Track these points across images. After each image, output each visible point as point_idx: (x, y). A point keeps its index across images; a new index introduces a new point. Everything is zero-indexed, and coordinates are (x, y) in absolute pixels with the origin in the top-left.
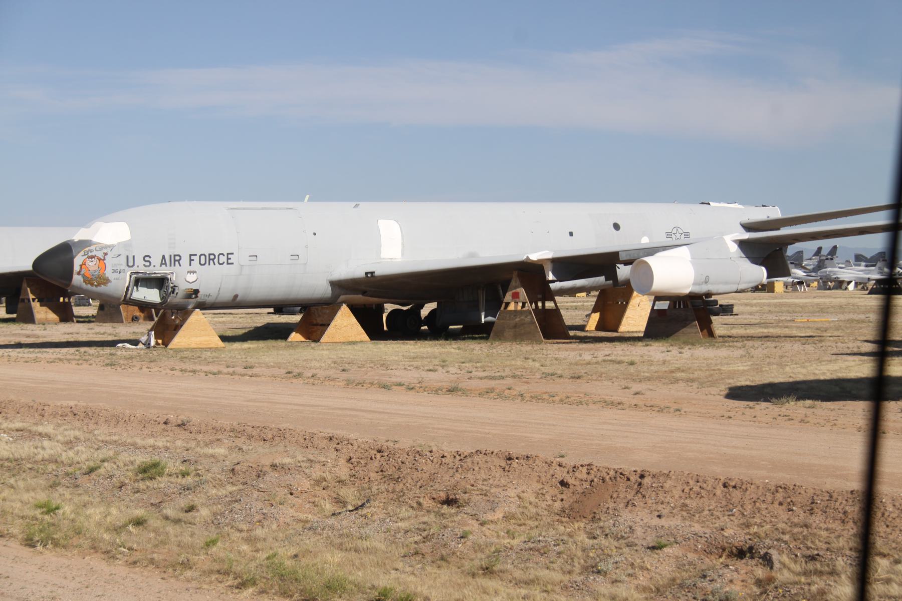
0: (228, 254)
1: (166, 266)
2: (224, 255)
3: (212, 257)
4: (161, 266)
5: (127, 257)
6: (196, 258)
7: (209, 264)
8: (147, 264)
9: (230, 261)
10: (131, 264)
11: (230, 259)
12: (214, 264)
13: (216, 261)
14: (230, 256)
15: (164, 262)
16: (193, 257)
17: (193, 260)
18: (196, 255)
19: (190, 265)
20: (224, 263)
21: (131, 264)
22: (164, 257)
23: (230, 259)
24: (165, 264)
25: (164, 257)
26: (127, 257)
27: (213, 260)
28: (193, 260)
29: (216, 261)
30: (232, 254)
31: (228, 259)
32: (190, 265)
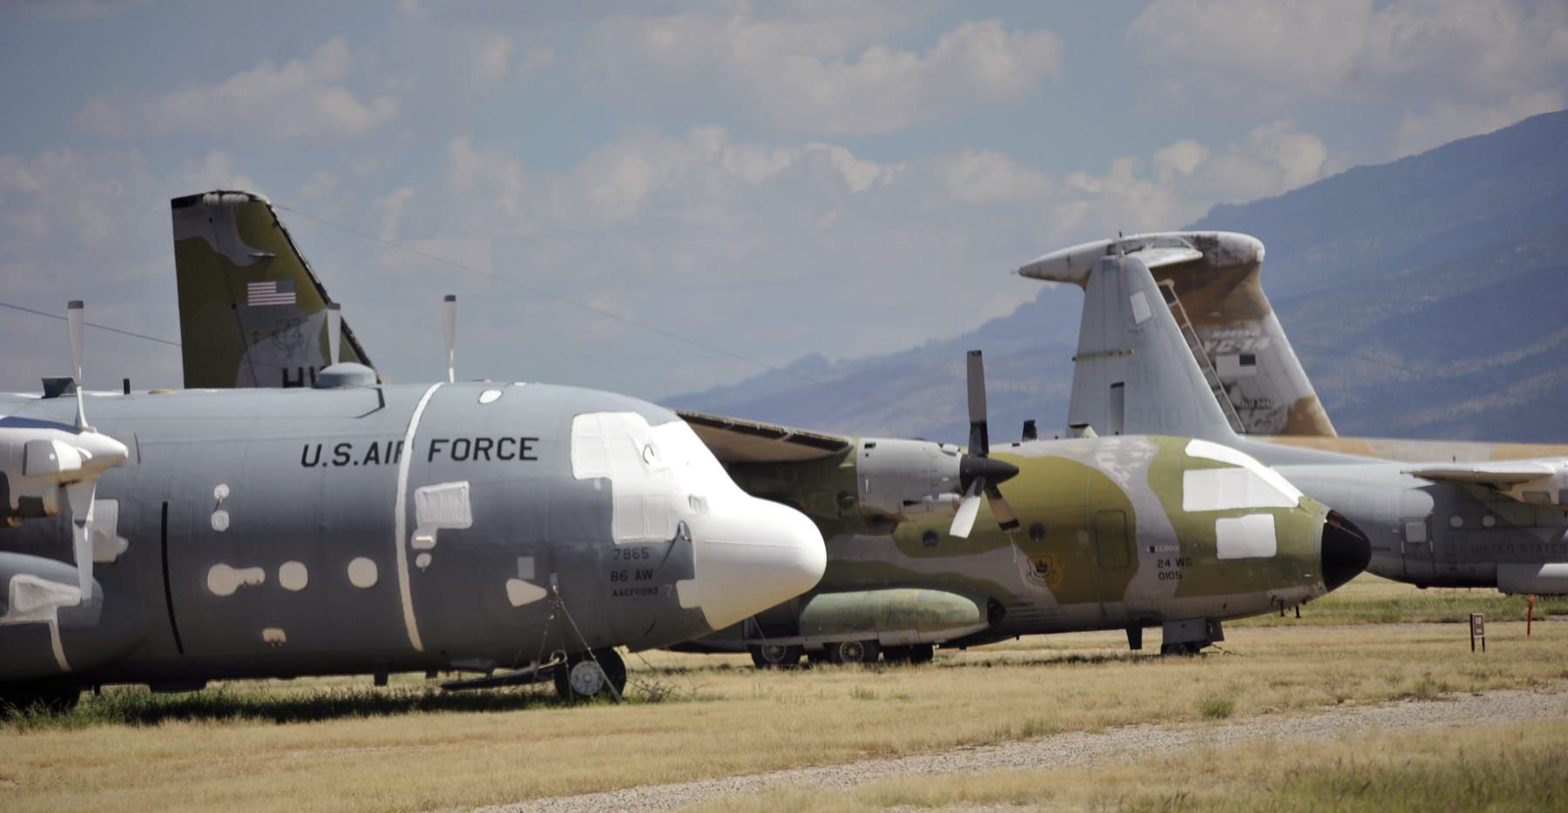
0: (523, 440)
1: (377, 462)
2: (513, 441)
3: (484, 444)
4: (365, 463)
5: (306, 448)
6: (446, 449)
7: (475, 457)
8: (342, 459)
9: (527, 453)
10: (310, 458)
11: (530, 448)
12: (488, 458)
13: (493, 452)
14: (527, 444)
15: (373, 454)
16: (437, 446)
17: (439, 450)
18: (447, 441)
19: (430, 459)
20: (513, 455)
21: (310, 458)
22: (375, 446)
23: (530, 448)
24: (377, 460)
25: (375, 446)
26: (306, 448)
27: (486, 450)
28: (439, 450)
29: (493, 452)
30: (536, 439)
31: (523, 448)
32: (430, 459)
